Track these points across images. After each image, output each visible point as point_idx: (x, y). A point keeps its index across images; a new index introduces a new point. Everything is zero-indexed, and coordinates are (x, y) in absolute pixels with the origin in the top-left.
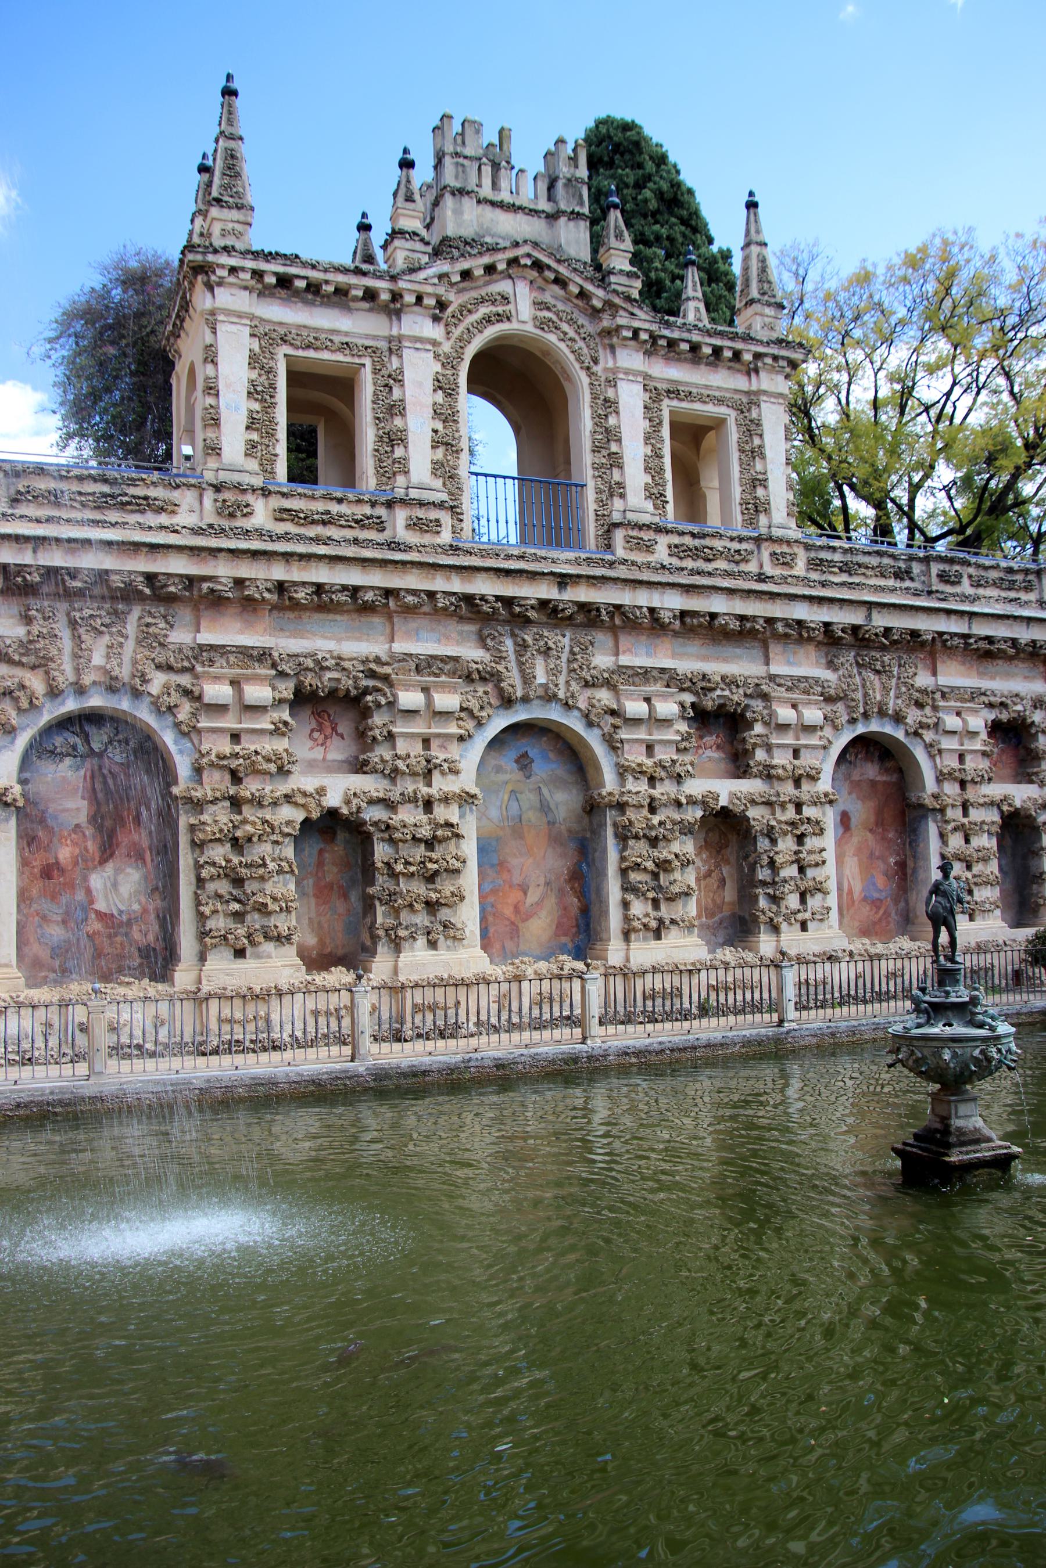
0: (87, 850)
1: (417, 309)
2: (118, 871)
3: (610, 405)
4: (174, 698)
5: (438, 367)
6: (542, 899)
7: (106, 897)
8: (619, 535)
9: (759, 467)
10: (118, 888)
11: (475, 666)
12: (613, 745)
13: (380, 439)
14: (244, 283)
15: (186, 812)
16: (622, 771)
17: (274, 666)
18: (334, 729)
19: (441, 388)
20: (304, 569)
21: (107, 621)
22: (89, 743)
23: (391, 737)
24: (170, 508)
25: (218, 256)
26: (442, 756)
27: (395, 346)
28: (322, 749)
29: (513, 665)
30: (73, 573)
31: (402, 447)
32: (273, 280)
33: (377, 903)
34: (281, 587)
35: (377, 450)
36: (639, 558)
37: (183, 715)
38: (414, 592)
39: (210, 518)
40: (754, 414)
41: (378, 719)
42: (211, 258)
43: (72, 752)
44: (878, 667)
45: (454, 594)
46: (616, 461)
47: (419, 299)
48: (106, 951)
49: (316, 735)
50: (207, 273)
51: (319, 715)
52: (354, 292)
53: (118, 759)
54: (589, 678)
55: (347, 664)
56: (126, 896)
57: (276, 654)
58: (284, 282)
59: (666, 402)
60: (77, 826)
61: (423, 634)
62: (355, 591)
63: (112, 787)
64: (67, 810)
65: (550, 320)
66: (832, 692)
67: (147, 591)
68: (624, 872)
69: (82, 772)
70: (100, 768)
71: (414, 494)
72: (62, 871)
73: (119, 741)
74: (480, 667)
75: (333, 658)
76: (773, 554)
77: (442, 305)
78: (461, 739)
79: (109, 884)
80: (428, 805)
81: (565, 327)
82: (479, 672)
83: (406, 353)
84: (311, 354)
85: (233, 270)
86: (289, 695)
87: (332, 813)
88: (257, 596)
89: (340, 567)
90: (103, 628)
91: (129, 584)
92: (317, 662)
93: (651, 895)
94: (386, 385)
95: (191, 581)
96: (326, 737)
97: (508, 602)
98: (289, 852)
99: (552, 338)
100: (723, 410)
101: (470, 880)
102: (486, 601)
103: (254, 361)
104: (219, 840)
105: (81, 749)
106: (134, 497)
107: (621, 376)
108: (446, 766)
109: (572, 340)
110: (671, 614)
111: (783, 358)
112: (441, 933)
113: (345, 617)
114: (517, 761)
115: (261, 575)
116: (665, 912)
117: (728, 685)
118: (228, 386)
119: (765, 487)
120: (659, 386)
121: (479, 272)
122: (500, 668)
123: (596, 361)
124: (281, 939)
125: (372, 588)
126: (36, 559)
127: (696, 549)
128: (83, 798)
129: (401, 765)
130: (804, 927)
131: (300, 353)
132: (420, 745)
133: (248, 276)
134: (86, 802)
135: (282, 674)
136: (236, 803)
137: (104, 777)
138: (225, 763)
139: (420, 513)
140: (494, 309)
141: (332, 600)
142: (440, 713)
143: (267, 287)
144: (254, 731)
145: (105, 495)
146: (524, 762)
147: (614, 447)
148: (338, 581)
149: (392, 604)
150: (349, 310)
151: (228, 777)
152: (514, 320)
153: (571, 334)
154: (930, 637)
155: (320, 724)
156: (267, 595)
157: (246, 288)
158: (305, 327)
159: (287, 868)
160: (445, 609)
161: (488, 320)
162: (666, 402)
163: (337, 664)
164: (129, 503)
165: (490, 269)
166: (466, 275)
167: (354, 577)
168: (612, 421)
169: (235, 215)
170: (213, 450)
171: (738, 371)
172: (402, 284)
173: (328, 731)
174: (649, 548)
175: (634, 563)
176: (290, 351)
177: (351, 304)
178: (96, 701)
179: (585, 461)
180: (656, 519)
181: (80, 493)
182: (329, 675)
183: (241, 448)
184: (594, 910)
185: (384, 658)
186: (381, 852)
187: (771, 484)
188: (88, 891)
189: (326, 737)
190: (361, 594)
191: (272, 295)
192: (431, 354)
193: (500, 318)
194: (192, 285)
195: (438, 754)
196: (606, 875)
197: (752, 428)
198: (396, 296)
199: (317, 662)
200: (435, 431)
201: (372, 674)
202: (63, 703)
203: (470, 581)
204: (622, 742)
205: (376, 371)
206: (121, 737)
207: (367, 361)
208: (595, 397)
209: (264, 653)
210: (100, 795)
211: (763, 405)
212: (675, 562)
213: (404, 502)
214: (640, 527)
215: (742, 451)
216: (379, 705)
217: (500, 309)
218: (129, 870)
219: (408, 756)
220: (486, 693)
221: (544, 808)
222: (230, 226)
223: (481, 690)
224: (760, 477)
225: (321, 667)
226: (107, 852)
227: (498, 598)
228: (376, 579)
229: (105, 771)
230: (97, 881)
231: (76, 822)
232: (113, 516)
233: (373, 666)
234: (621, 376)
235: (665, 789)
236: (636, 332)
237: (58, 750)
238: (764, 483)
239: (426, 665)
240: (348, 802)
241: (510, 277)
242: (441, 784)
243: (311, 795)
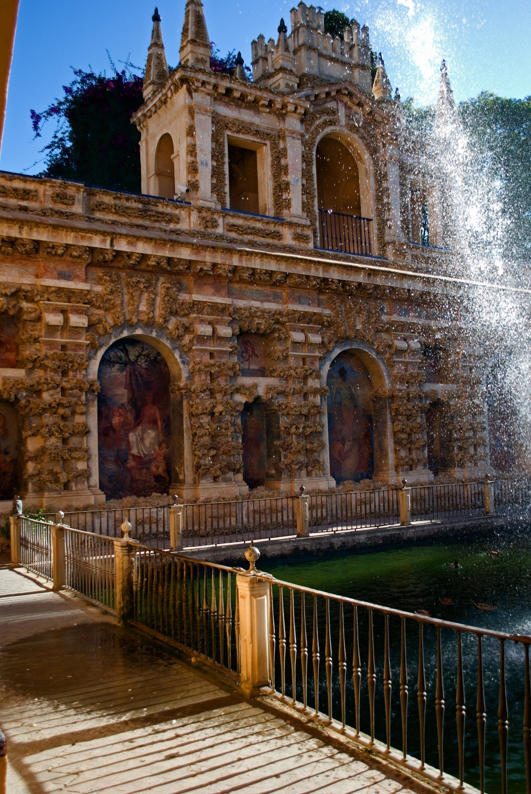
0: (127, 418)
2: (144, 431)
6: (351, 449)
7: (137, 446)
8: (390, 250)
10: (144, 441)
11: (325, 318)
12: (390, 365)
14: (208, 92)
15: (187, 397)
16: (394, 379)
17: (230, 315)
20: (248, 260)
21: (146, 285)
22: (128, 356)
23: (286, 357)
25: (197, 74)
27: (281, 136)
28: (247, 363)
30: (129, 255)
31: (287, 194)
32: (224, 92)
33: (281, 450)
34: (235, 270)
38: (300, 276)
42: (193, 75)
43: (119, 362)
45: (319, 278)
46: (387, 207)
47: (296, 108)
48: (137, 478)
49: (245, 355)
50: (189, 83)
51: (245, 343)
52: (262, 102)
53: (144, 365)
56: (148, 445)
57: (231, 309)
60: (122, 404)
61: (302, 300)
62: (271, 273)
63: (140, 382)
64: (118, 395)
68: (395, 433)
69: (125, 373)
70: (134, 370)
71: (295, 220)
72: (114, 430)
77: (305, 114)
78: (321, 359)
79: (139, 439)
80: (305, 396)
83: (288, 139)
84: (241, 136)
85: (204, 83)
86: (237, 331)
87: (258, 398)
88: (225, 274)
89: (265, 260)
90: (145, 290)
93: (409, 446)
97: (344, 283)
98: (239, 421)
101: (326, 437)
104: (204, 414)
105: (124, 359)
108: (314, 373)
112: (311, 466)
113: (263, 288)
114: (339, 372)
115: (227, 263)
116: (414, 455)
118: (202, 151)
121: (323, 96)
124: (236, 471)
125: (281, 272)
126: (112, 245)
128: (125, 388)
130: (476, 464)
131: (235, 135)
132: (301, 363)
133: (211, 87)
134: (126, 391)
135: (234, 319)
136: (212, 393)
137: (136, 376)
138: (208, 369)
139: (299, 230)
141: (260, 278)
142: (312, 344)
144: (221, 352)
146: (343, 373)
148: (265, 268)
151: (209, 377)
155: (246, 349)
157: (209, 94)
158: (237, 120)
159: (238, 430)
161: (326, 123)
164: (154, 216)
165: (328, 94)
166: (316, 96)
167: (273, 266)
170: (193, 187)
173: (250, 353)
176: (229, 133)
177: (261, 109)
179: (368, 207)
182: (257, 321)
184: (377, 455)
186: (284, 421)
188: (128, 442)
189: (249, 356)
190: (274, 276)
191: (220, 100)
192: (300, 142)
193: (332, 123)
194: (177, 89)
196: (386, 435)
198: (284, 106)
200: (303, 185)
201: (277, 322)
202: (122, 332)
203: (327, 272)
204: (394, 362)
206: (144, 353)
207: (268, 143)
210: (134, 387)
213: (291, 224)
216: (280, 339)
218: (150, 431)
221: (352, 398)
226: (138, 419)
227: (340, 281)
228: (283, 267)
229: (137, 373)
230: (132, 437)
231: (122, 402)
232: (147, 223)
235: (414, 389)
237: (112, 359)
239: (304, 317)
240: (267, 393)
241: (336, 100)
243: (249, 389)
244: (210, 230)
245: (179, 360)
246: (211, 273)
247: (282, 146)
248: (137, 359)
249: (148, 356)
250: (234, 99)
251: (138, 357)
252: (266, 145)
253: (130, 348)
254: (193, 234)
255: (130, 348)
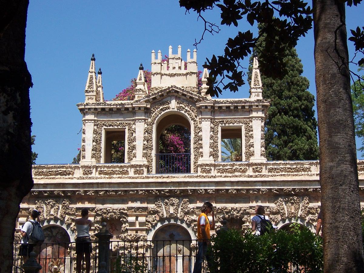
1: (140, 111)
3: (200, 129)
4: (70, 222)
5: (146, 126)
8: (199, 169)
9: (251, 141)
13: (129, 148)
17: (96, 212)
18: (115, 228)
19: (147, 132)
21: (54, 202)
22: (52, 234)
24: (72, 173)
26: (141, 235)
29: (164, 208)
30: (45, 192)
35: (128, 151)
36: (205, 174)
37: (71, 226)
39: (82, 175)
40: (251, 124)
41: (124, 225)
44: (292, 201)
54: (186, 211)
55: (114, 211)
58: (103, 109)
59: (220, 125)
62: (116, 192)
65: (182, 107)
66: (274, 211)
67: (63, 195)
73: (60, 233)
74: (153, 209)
75: (112, 209)
76: (253, 169)
81: (187, 108)
82: (153, 211)
83: (136, 123)
84: (111, 127)
85: (89, 109)
88: (90, 194)
91: (59, 194)
92: (107, 211)
94: (131, 133)
95: (74, 192)
96: (113, 231)
99: (183, 112)
100: (241, 124)
102: (154, 191)
103: (95, 132)
106: (62, 171)
107: (203, 120)
109: (189, 111)
110: (212, 191)
111: (260, 105)
114: (170, 236)
117: (234, 211)
119: (253, 147)
120: (217, 121)
122: (158, 209)
123: (196, 117)
127: (226, 169)
129: (129, 237)
131: (108, 128)
140: (164, 106)
143: (99, 111)
145: (56, 171)
147: (200, 142)
149: (127, 193)
150: (122, 114)
152: (171, 109)
153: (189, 109)
154: (312, 190)
156: (93, 194)
160: (142, 194)
162: (220, 125)
163: (112, 211)
168: (200, 134)
169: (91, 94)
171: (246, 111)
172: (134, 105)
173: (114, 229)
174: (209, 171)
175: (203, 176)
177: (122, 112)
178: (52, 223)
180: (213, 162)
181: (50, 171)
182: (110, 214)
183: (90, 155)
185: (126, 208)
187: (254, 146)
191: (101, 113)
192: (144, 123)
193: (166, 108)
195: (140, 234)
197: (249, 129)
199: (107, 211)
205: (129, 130)
206: (60, 232)
207: (127, 127)
208: (195, 127)
209: (93, 209)
211: (253, 121)
212: (219, 174)
214: (207, 165)
215: (246, 137)
217: (166, 106)
219: (131, 235)
220: (155, 217)
222: (90, 97)
223: (154, 216)
224: (251, 144)
225: (108, 212)
227: (157, 190)
233: (121, 211)
234: (203, 120)
236: (206, 107)
238: (252, 146)
242: (141, 243)
244: (89, 176)
245: (69, 234)
246: (83, 194)
247: (134, 127)
248: (56, 235)
249: (62, 233)
250: (107, 112)
251: (57, 233)
252: (126, 128)
253: (53, 230)
254: (81, 178)
255: (53, 230)
